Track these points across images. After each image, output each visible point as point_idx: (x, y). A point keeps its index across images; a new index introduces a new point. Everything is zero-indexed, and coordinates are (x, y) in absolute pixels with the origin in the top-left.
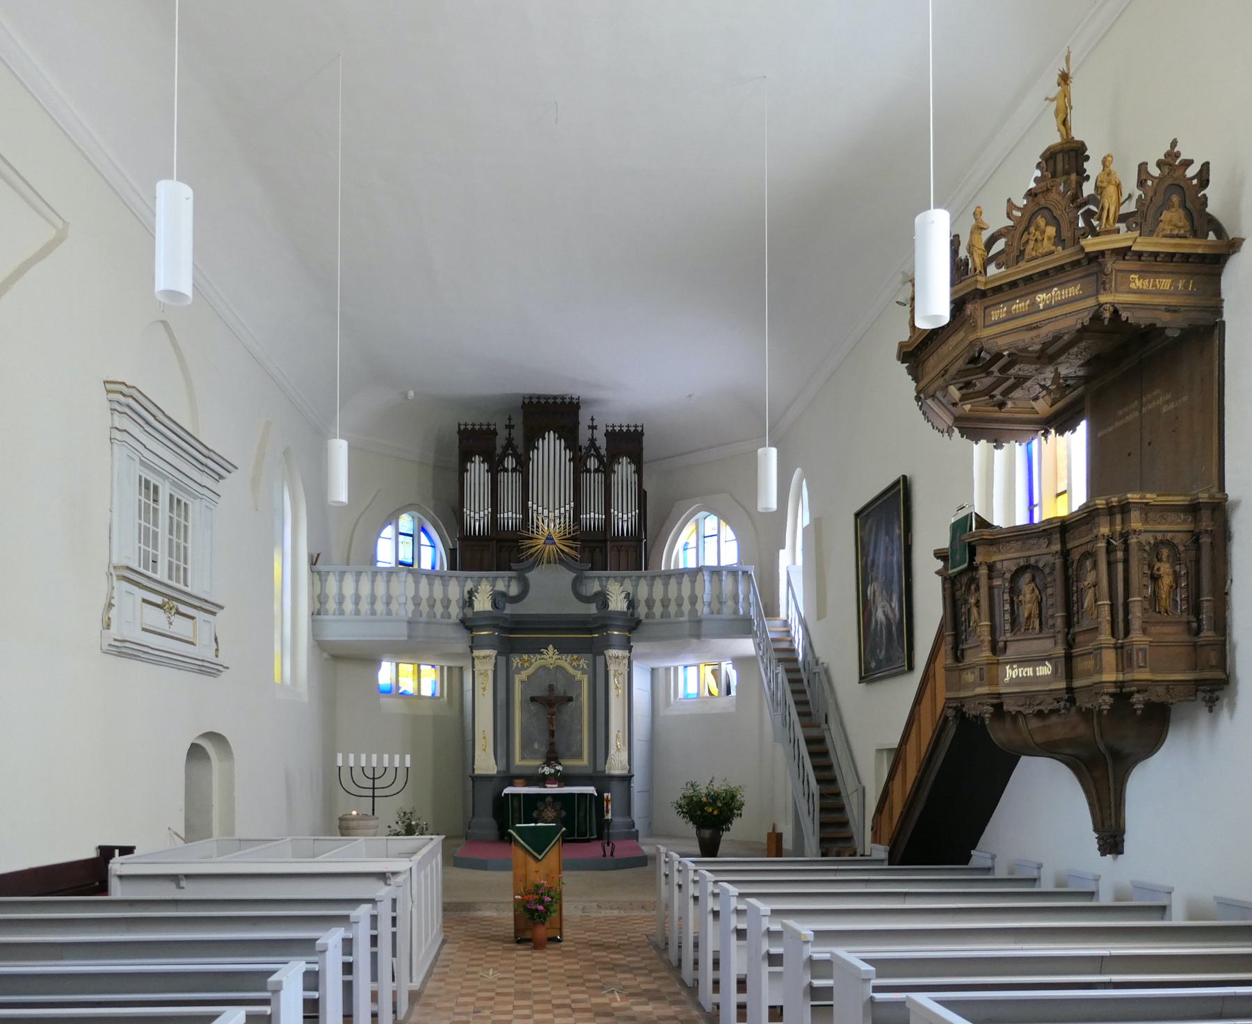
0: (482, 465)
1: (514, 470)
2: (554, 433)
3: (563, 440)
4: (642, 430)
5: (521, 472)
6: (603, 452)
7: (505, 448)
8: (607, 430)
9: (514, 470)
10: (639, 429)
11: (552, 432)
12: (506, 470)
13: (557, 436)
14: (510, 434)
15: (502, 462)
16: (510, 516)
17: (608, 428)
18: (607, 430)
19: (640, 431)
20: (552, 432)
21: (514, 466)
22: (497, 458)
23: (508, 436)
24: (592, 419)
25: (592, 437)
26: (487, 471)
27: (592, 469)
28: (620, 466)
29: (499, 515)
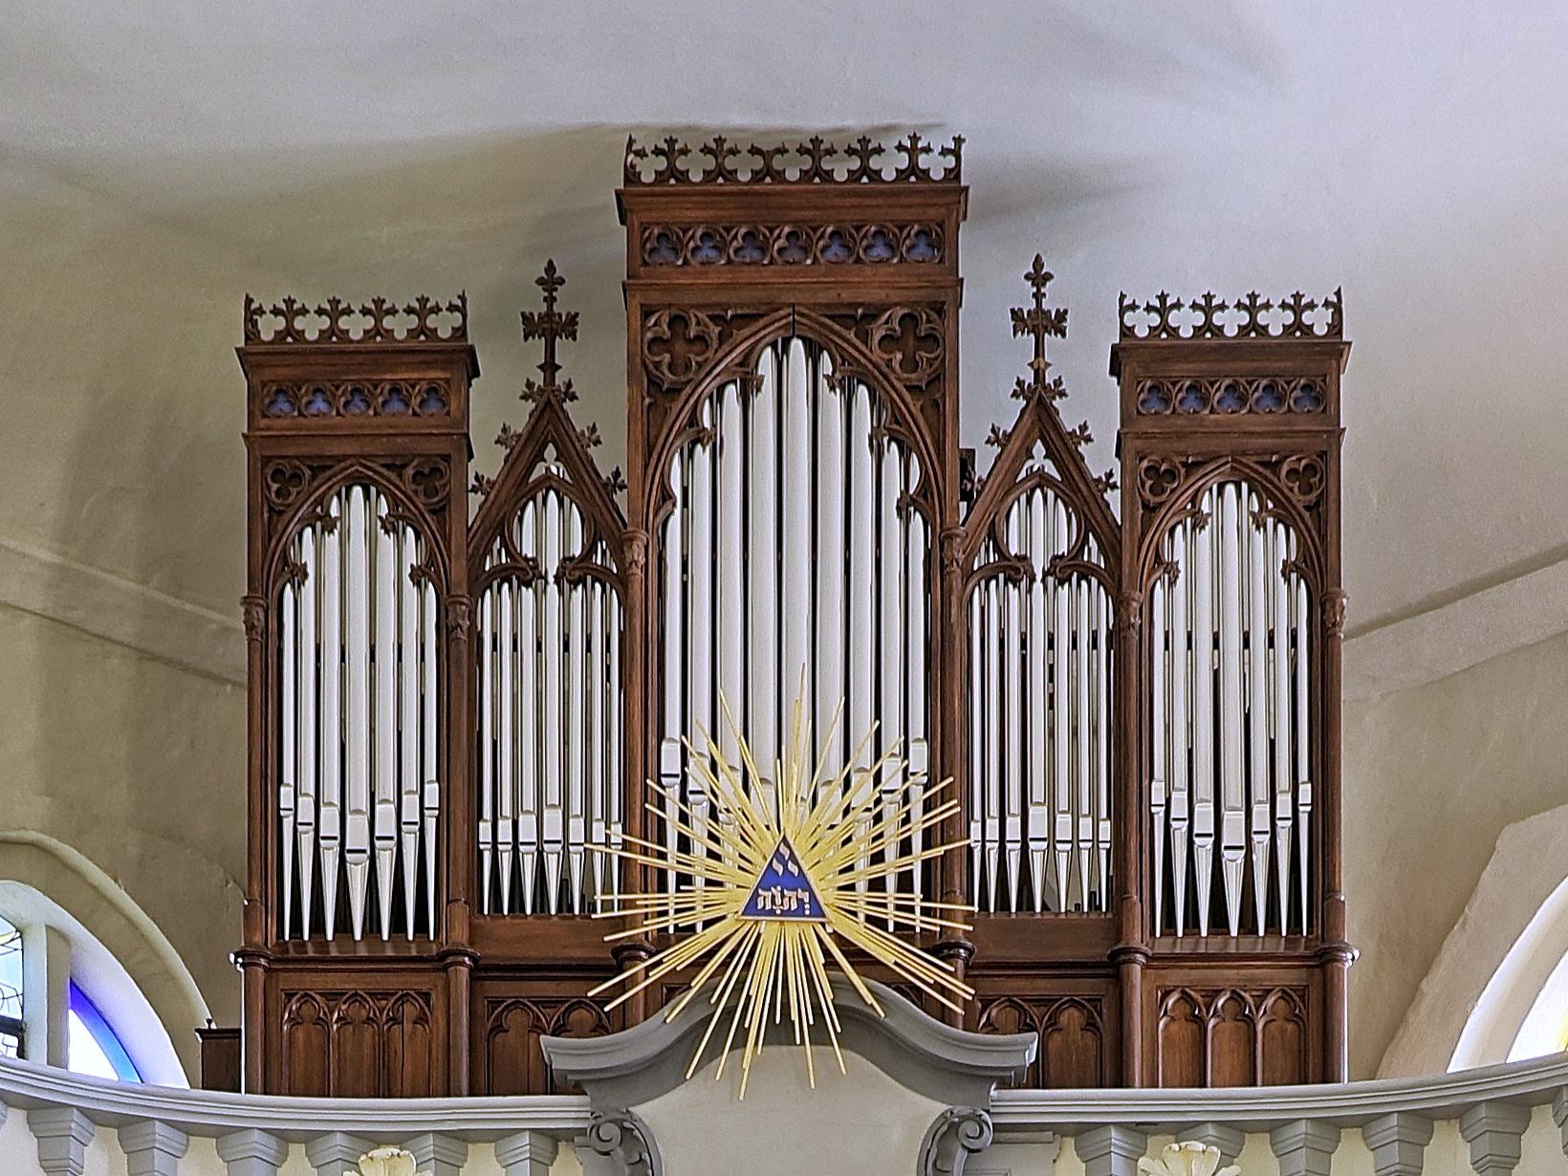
0: (387, 542)
1: (574, 572)
2: (813, 353)
3: (862, 391)
4: (1336, 328)
5: (621, 582)
6: (1100, 459)
7: (524, 449)
8: (1126, 332)
9: (574, 572)
10: (1319, 321)
11: (797, 346)
12: (525, 572)
13: (826, 365)
14: (550, 367)
15: (500, 524)
16: (553, 830)
17: (1129, 318)
18: (1126, 332)
19: (1321, 330)
20: (797, 346)
21: (577, 550)
22: (475, 500)
23: (539, 379)
24: (1039, 278)
25: (1039, 375)
26: (418, 576)
27: (1039, 565)
28: (1204, 536)
29: (485, 831)
